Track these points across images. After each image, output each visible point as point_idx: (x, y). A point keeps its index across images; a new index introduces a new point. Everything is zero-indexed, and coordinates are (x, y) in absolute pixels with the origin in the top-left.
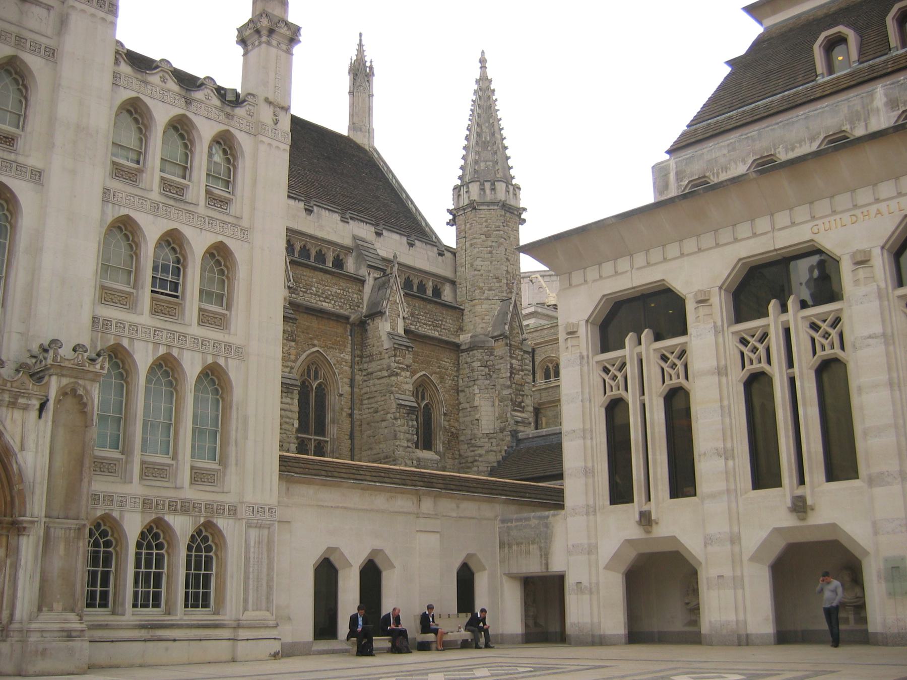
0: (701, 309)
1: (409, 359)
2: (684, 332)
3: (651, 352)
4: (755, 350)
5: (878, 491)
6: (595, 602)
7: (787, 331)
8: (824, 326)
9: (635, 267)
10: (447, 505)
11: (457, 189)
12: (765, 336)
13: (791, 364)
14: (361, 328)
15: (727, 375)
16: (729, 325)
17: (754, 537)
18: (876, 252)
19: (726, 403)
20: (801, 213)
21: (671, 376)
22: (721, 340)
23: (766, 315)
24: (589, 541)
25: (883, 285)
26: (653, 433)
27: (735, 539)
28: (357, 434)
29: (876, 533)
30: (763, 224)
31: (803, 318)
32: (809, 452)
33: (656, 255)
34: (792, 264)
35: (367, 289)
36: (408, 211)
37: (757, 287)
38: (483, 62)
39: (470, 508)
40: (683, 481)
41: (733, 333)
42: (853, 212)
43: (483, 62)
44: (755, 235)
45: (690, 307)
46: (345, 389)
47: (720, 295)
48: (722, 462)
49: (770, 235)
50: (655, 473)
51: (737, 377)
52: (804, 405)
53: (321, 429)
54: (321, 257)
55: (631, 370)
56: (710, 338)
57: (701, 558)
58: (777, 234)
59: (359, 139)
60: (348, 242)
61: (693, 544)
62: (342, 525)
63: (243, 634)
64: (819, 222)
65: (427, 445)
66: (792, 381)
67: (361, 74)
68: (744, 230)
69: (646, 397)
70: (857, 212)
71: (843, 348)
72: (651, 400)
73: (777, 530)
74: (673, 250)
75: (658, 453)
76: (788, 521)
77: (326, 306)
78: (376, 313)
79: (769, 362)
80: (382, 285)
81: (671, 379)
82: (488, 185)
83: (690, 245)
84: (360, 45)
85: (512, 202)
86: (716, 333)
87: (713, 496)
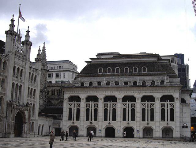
5: (99, 122)
7: (92, 104)
12: (89, 104)
17: (86, 126)
20: (95, 92)
24: (65, 125)
27: (84, 126)
30: (91, 92)
33: (78, 92)
38: (44, 44)
40: (78, 119)
43: (44, 44)
51: (86, 108)
61: (79, 126)
63: (36, 134)
66: (92, 110)
68: (89, 92)
74: (80, 92)
82: (44, 66)
83: (82, 92)
87: (82, 121)
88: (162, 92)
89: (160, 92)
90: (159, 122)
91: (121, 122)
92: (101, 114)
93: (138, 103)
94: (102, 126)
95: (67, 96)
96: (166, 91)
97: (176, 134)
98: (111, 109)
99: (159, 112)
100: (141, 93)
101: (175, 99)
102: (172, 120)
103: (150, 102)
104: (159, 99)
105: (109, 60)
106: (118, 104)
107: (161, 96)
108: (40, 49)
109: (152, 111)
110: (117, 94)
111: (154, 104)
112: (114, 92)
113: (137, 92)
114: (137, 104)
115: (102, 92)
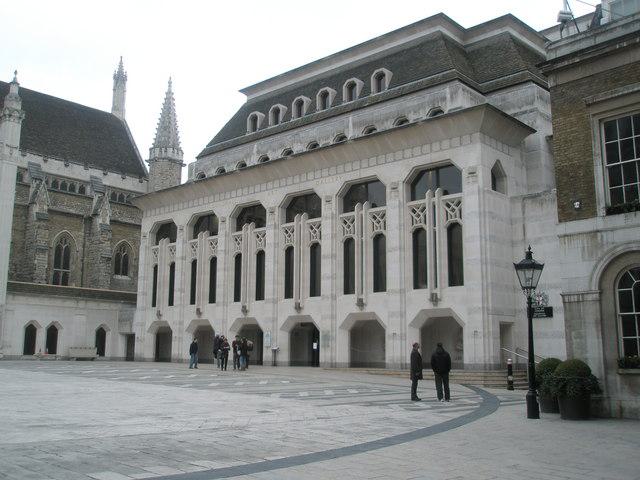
1: (110, 235)
6: (145, 346)
10: (92, 305)
11: (151, 149)
14: (90, 220)
16: (190, 239)
24: (143, 322)
28: (85, 269)
35: (95, 201)
36: (136, 156)
38: (170, 83)
39: (104, 306)
43: (170, 83)
46: (81, 248)
53: (66, 266)
54: (72, 188)
59: (117, 115)
60: (87, 179)
62: (42, 312)
65: (125, 273)
67: (120, 79)
77: (72, 211)
78: (96, 215)
80: (100, 201)
84: (121, 63)
85: (176, 157)
95: (148, 225)
97: (477, 348)
101: (465, 175)
102: (456, 278)
105: (292, 82)
108: (15, 78)
109: (379, 241)
113: (325, 172)
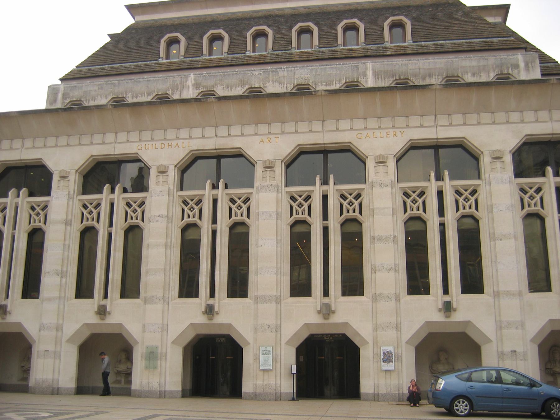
0: (62, 181)
2: (49, 194)
3: (25, 203)
4: (91, 213)
5: (149, 306)
7: (112, 205)
8: (134, 206)
9: (25, 146)
12: (98, 205)
13: (111, 225)
15: (71, 225)
16: (78, 195)
18: (172, 168)
19: (67, 242)
20: (134, 136)
21: (35, 220)
22: (71, 203)
23: (101, 192)
25: (172, 188)
26: (17, 255)
27: (59, 328)
29: (144, 331)
30: (110, 137)
31: (123, 198)
32: (113, 279)
33: (39, 142)
34: (123, 164)
37: (100, 175)
41: (79, 200)
42: (163, 142)
44: (104, 143)
45: (55, 179)
47: (76, 176)
48: (59, 279)
49: (113, 145)
50: (14, 281)
51: (77, 227)
52: (115, 250)
55: (9, 212)
56: (65, 201)
57: (36, 338)
58: (117, 145)
61: (31, 329)
64: (143, 144)
66: (110, 235)
68: (98, 138)
69: (16, 232)
70: (166, 142)
71: (143, 220)
72: (19, 233)
73: (87, 325)
74: (51, 141)
75: (18, 268)
76: (93, 319)
79: (98, 221)
81: (35, 222)
83: (63, 140)
86: (69, 198)
87: (49, 300)
88: (522, 122)
89: (508, 122)
90: (520, 294)
91: (278, 300)
92: (160, 258)
93: (382, 185)
94: (164, 328)
96: (543, 114)
98: (218, 226)
99: (516, 238)
100: (393, 127)
103: (452, 178)
104: (508, 159)
106: (261, 194)
107: (513, 142)
110: (258, 138)
111: (474, 192)
112: (236, 130)
114: (377, 190)
115: (171, 134)
